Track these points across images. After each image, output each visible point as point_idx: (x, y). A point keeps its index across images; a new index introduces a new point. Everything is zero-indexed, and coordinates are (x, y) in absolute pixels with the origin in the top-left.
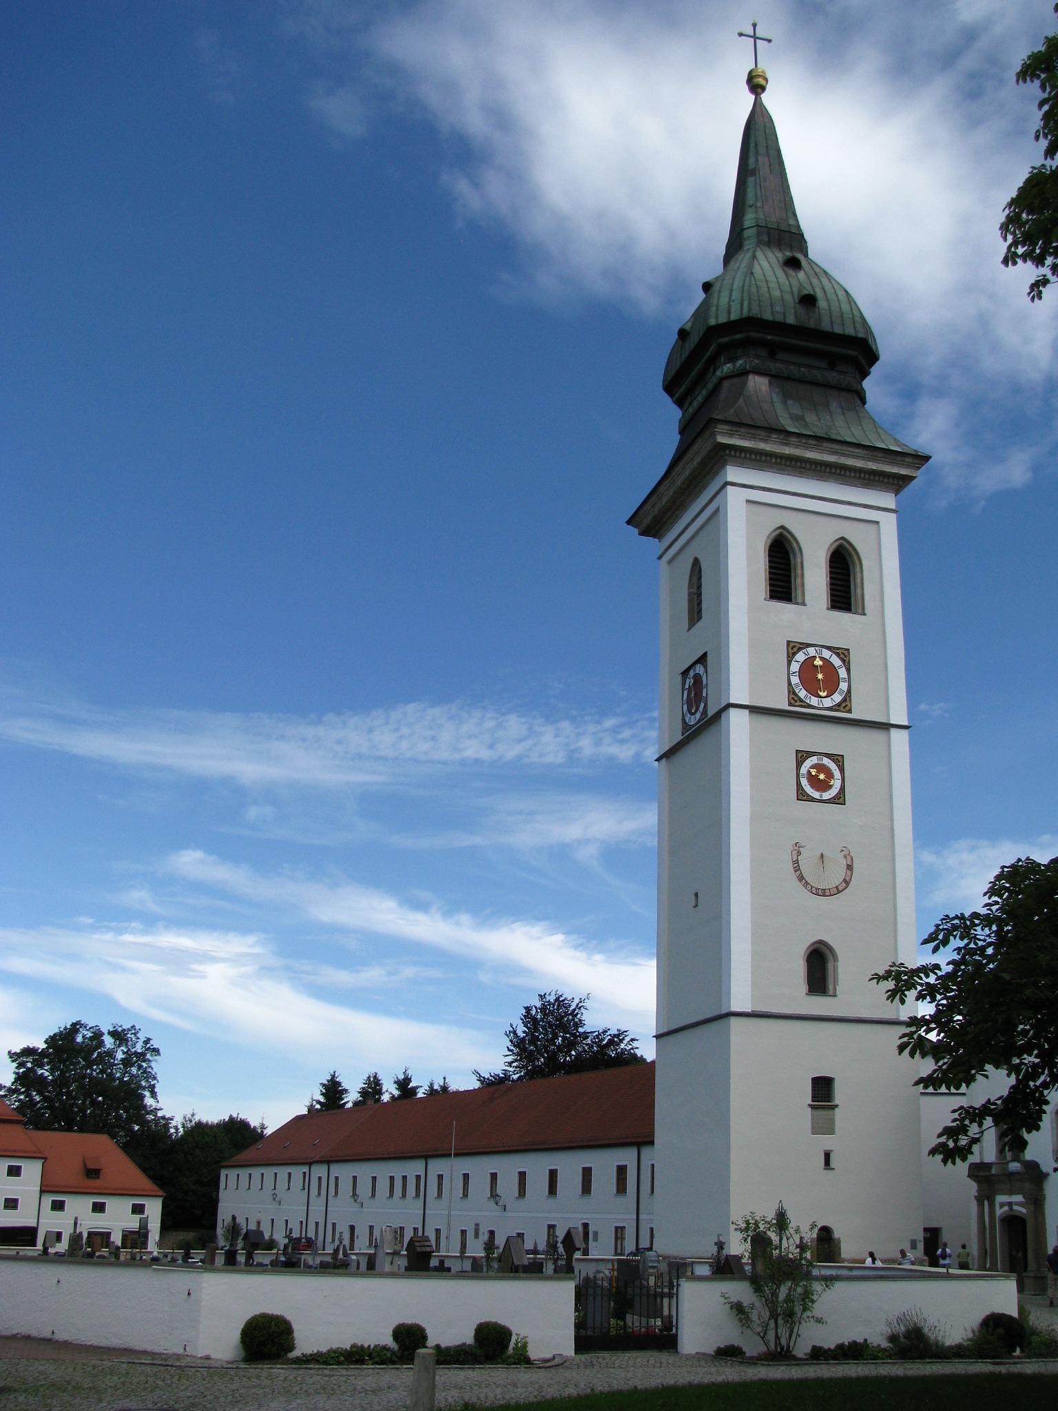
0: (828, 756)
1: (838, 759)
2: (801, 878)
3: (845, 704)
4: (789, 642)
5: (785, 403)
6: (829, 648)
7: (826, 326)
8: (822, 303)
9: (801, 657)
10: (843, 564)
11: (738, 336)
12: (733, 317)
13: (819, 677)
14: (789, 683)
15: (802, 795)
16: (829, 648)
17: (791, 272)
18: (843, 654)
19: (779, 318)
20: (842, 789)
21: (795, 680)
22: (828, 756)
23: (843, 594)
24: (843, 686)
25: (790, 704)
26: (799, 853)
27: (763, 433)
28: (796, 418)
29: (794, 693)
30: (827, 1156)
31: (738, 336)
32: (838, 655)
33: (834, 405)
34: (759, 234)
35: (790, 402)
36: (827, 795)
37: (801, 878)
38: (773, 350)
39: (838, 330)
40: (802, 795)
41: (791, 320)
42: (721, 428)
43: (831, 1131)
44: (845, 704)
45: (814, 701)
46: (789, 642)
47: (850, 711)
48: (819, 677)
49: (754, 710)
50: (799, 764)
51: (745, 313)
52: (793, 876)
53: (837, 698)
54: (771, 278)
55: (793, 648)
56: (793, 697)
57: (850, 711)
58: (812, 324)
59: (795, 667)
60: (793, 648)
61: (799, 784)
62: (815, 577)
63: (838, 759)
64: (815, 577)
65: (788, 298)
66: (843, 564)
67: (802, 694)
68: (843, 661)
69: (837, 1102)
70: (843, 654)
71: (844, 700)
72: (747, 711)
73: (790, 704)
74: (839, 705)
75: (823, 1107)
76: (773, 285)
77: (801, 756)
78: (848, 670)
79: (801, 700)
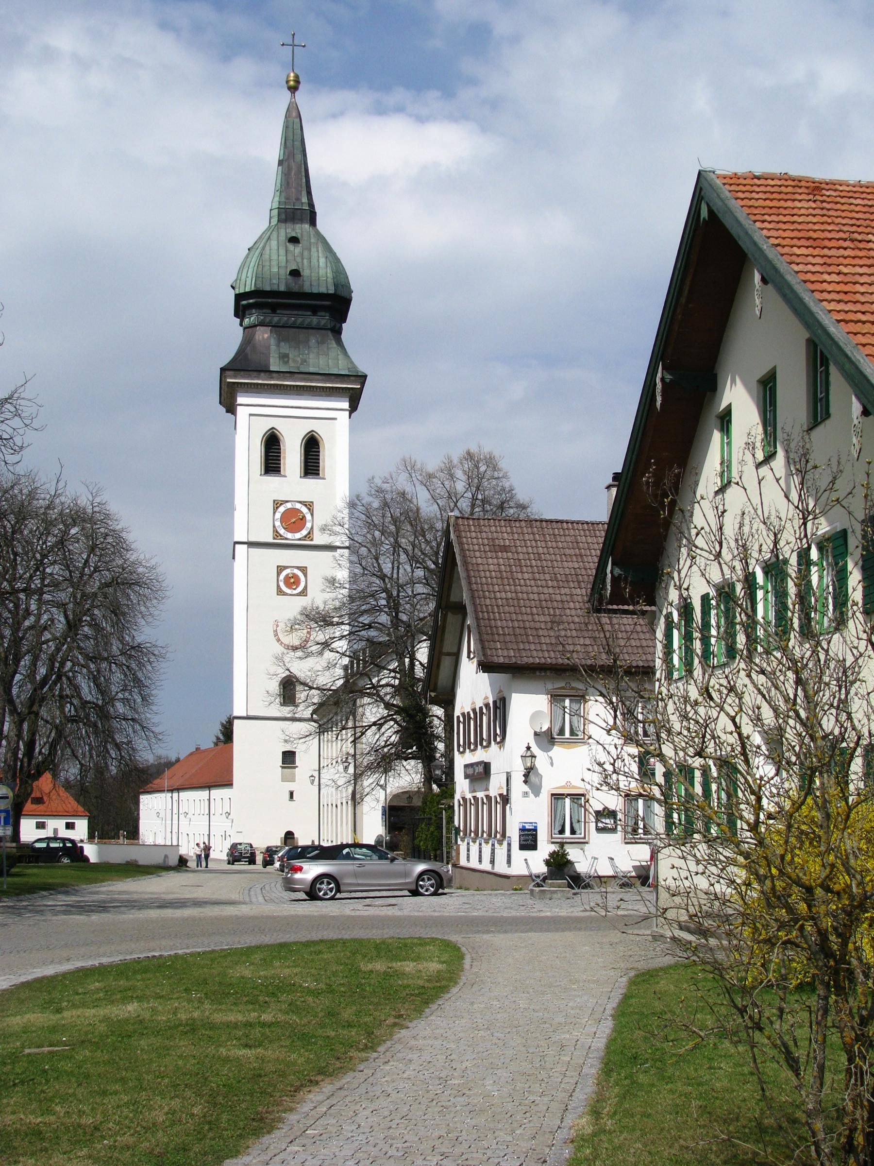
0: (298, 568)
1: (304, 570)
2: (278, 640)
3: (309, 536)
4: (274, 501)
5: (278, 346)
6: (300, 502)
7: (307, 289)
8: (305, 273)
9: (282, 509)
10: (312, 446)
11: (251, 301)
12: (248, 290)
13: (293, 519)
14: (274, 526)
15: (280, 592)
16: (300, 502)
17: (291, 247)
18: (309, 505)
19: (275, 288)
20: (306, 587)
21: (278, 524)
22: (298, 568)
23: (311, 465)
24: (309, 525)
25: (274, 538)
26: (277, 626)
27: (255, 374)
28: (284, 357)
29: (277, 532)
30: (291, 794)
31: (251, 301)
32: (306, 505)
33: (313, 341)
34: (279, 215)
35: (282, 344)
36: (295, 592)
37: (278, 640)
38: (274, 308)
39: (315, 291)
40: (280, 592)
41: (282, 288)
42: (228, 373)
43: (292, 779)
44: (309, 536)
45: (289, 535)
46: (274, 501)
47: (312, 540)
48: (293, 519)
49: (251, 544)
50: (278, 575)
51: (253, 289)
52: (274, 639)
53: (304, 532)
54: (274, 257)
55: (277, 504)
56: (276, 534)
57: (312, 540)
58: (296, 289)
59: (278, 515)
60: (277, 504)
61: (278, 586)
62: (292, 456)
63: (304, 570)
64: (292, 456)
65: (282, 272)
66: (312, 446)
67: (282, 531)
68: (309, 509)
69: (297, 764)
70: (309, 505)
71: (309, 533)
72: (246, 546)
73: (274, 538)
74: (305, 536)
75: (289, 768)
76: (274, 263)
77: (280, 569)
78: (312, 515)
79: (281, 536)
